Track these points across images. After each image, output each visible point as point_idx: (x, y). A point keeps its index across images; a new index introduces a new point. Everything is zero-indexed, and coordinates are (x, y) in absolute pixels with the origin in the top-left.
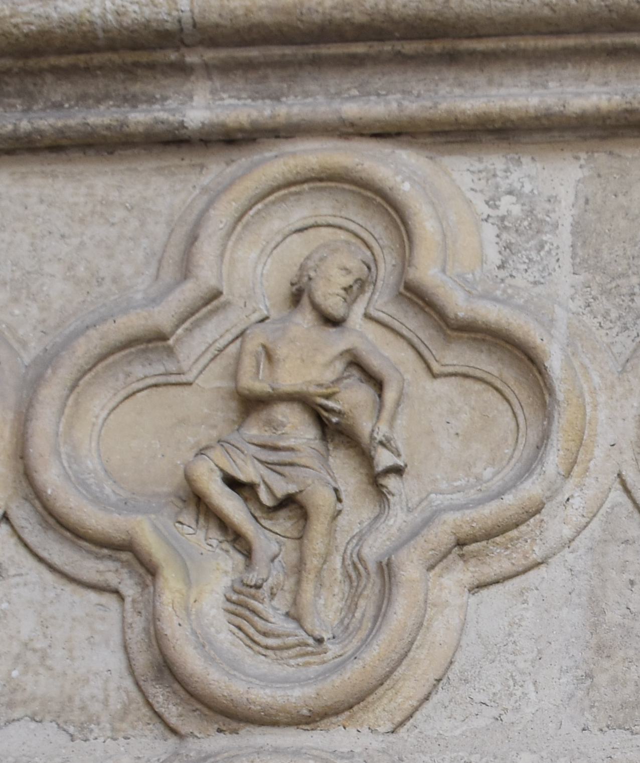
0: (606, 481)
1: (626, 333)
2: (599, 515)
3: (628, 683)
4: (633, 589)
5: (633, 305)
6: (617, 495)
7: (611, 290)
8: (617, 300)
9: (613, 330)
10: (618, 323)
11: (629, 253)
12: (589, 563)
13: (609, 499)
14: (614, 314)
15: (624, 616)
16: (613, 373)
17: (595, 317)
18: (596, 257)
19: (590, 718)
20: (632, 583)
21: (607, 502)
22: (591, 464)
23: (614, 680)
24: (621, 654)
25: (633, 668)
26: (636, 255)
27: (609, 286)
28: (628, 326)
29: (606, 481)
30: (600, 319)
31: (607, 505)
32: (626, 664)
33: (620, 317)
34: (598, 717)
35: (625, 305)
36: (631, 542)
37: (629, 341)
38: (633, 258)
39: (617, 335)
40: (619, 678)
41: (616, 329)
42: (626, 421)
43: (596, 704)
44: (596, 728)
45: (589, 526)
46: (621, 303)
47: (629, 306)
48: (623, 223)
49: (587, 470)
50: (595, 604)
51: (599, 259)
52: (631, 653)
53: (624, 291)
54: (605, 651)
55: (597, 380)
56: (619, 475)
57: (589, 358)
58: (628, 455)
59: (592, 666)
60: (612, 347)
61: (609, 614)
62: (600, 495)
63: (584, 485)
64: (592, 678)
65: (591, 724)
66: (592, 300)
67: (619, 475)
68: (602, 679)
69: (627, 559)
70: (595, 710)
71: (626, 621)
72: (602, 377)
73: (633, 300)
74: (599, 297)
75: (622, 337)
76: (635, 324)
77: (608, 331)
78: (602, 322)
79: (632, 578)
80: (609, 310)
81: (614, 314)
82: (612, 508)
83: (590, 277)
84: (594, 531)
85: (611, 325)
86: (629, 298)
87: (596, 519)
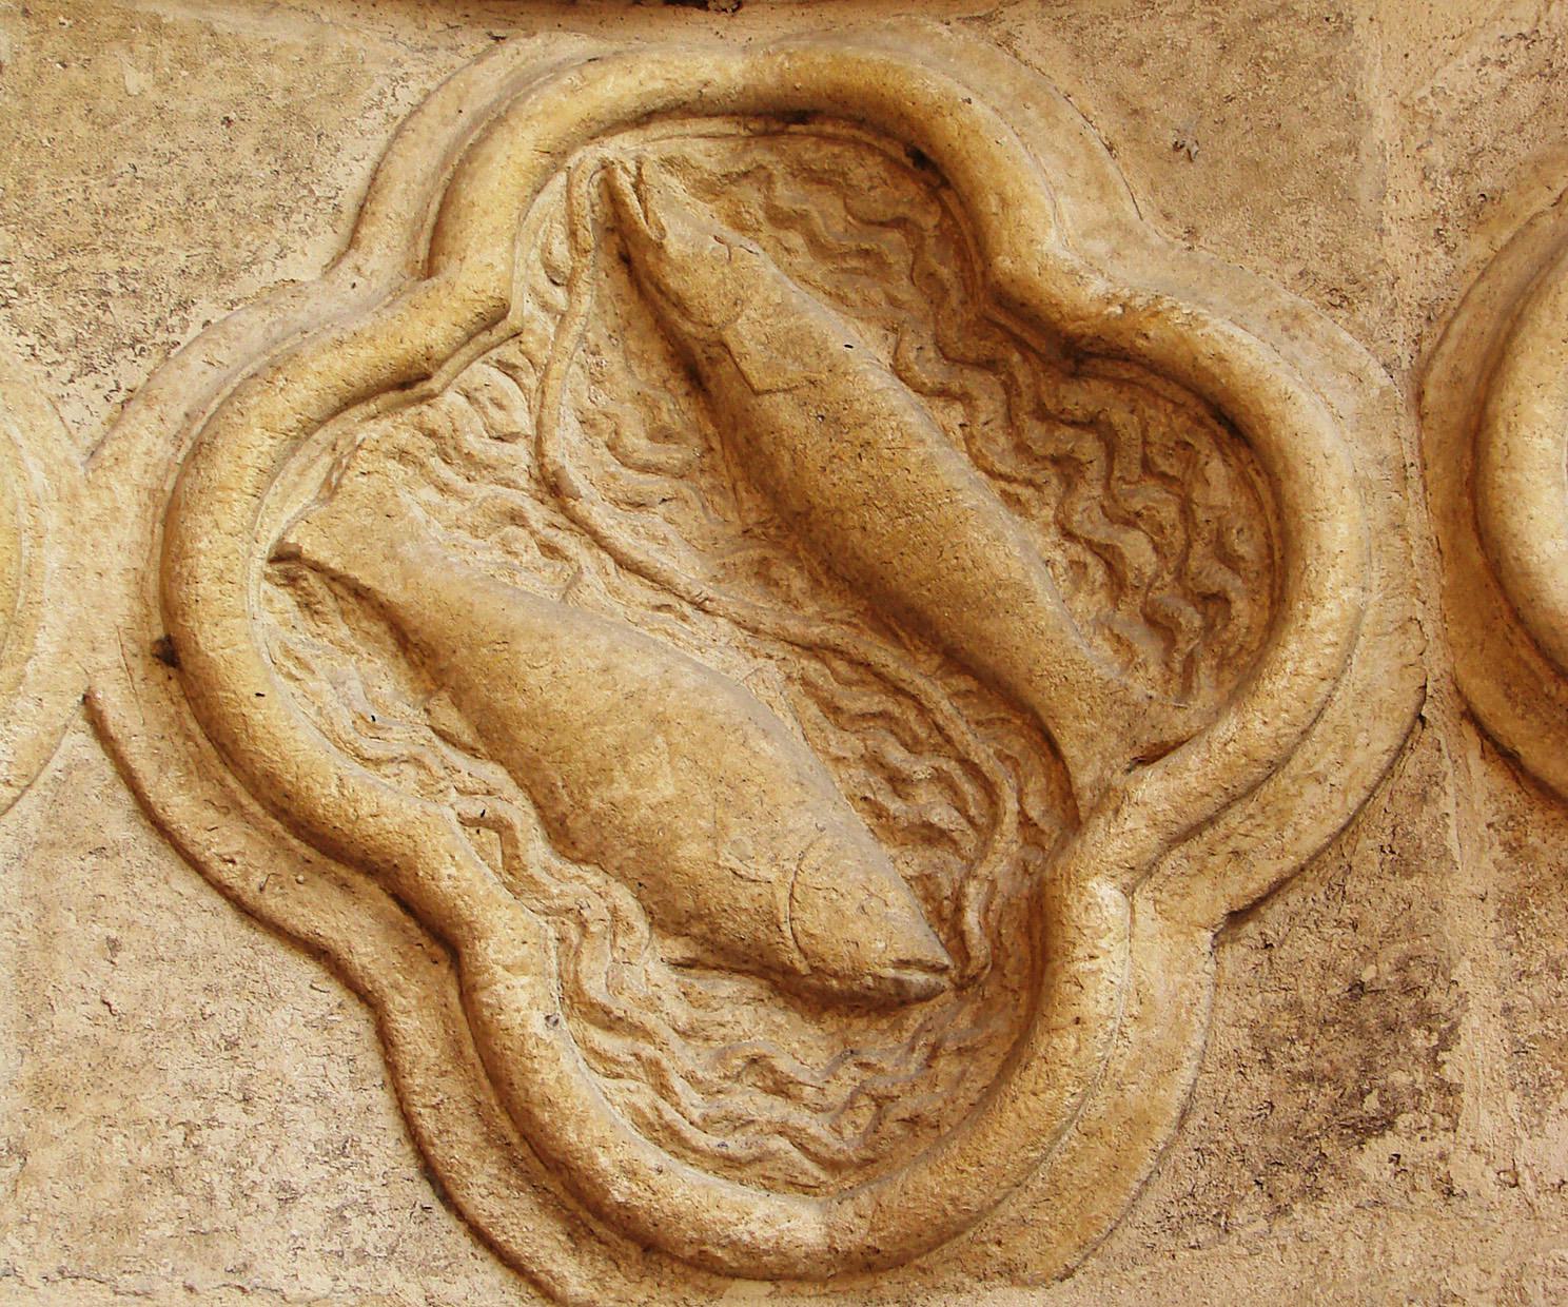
0: (59, 710)
1: (93, 378)
2: (39, 785)
3: (108, 1175)
4: (116, 960)
5: (107, 318)
6: (80, 744)
7: (56, 276)
8: (71, 301)
9: (62, 368)
10: (74, 355)
11: (95, 198)
12: (15, 891)
13: (61, 751)
14: (64, 333)
15: (94, 1020)
16: (73, 468)
17: (21, 333)
18: (21, 197)
19: (19, 1247)
20: (114, 945)
21: (56, 757)
22: (29, 668)
23: (75, 1164)
24: (89, 1105)
25: (118, 1140)
26: (112, 205)
27: (53, 267)
28: (96, 362)
29: (59, 710)
30: (33, 340)
31: (57, 763)
32: (102, 1130)
33: (77, 341)
34: (37, 1248)
35: (88, 317)
36: (109, 853)
37: (98, 396)
38: (106, 211)
39: (71, 381)
40: (87, 1161)
41: (70, 368)
42: (105, 580)
43: (34, 1217)
44: (35, 1273)
45: (16, 808)
46: (79, 308)
47: (97, 319)
48: (82, 130)
49: (20, 679)
50: (30, 986)
51: (30, 203)
52: (113, 1105)
53: (87, 283)
54: (53, 1096)
55: (39, 478)
56: (87, 700)
57: (19, 425)
58: (110, 656)
59: (23, 1128)
60: (60, 406)
61: (62, 1015)
62: (46, 739)
63: (13, 713)
64: (24, 1155)
65: (21, 1262)
66: (14, 294)
67: (87, 700)
68: (47, 1159)
69: (103, 892)
70: (31, 1230)
71: (100, 1032)
72: (48, 470)
73: (105, 307)
74: (31, 288)
75: (84, 385)
76: (110, 361)
77: (50, 369)
78: (37, 347)
79: (113, 934)
80: (54, 321)
81: (64, 333)
82: (68, 770)
83: (9, 239)
84: (26, 818)
85: (59, 357)
86: (98, 301)
87: (32, 792)
